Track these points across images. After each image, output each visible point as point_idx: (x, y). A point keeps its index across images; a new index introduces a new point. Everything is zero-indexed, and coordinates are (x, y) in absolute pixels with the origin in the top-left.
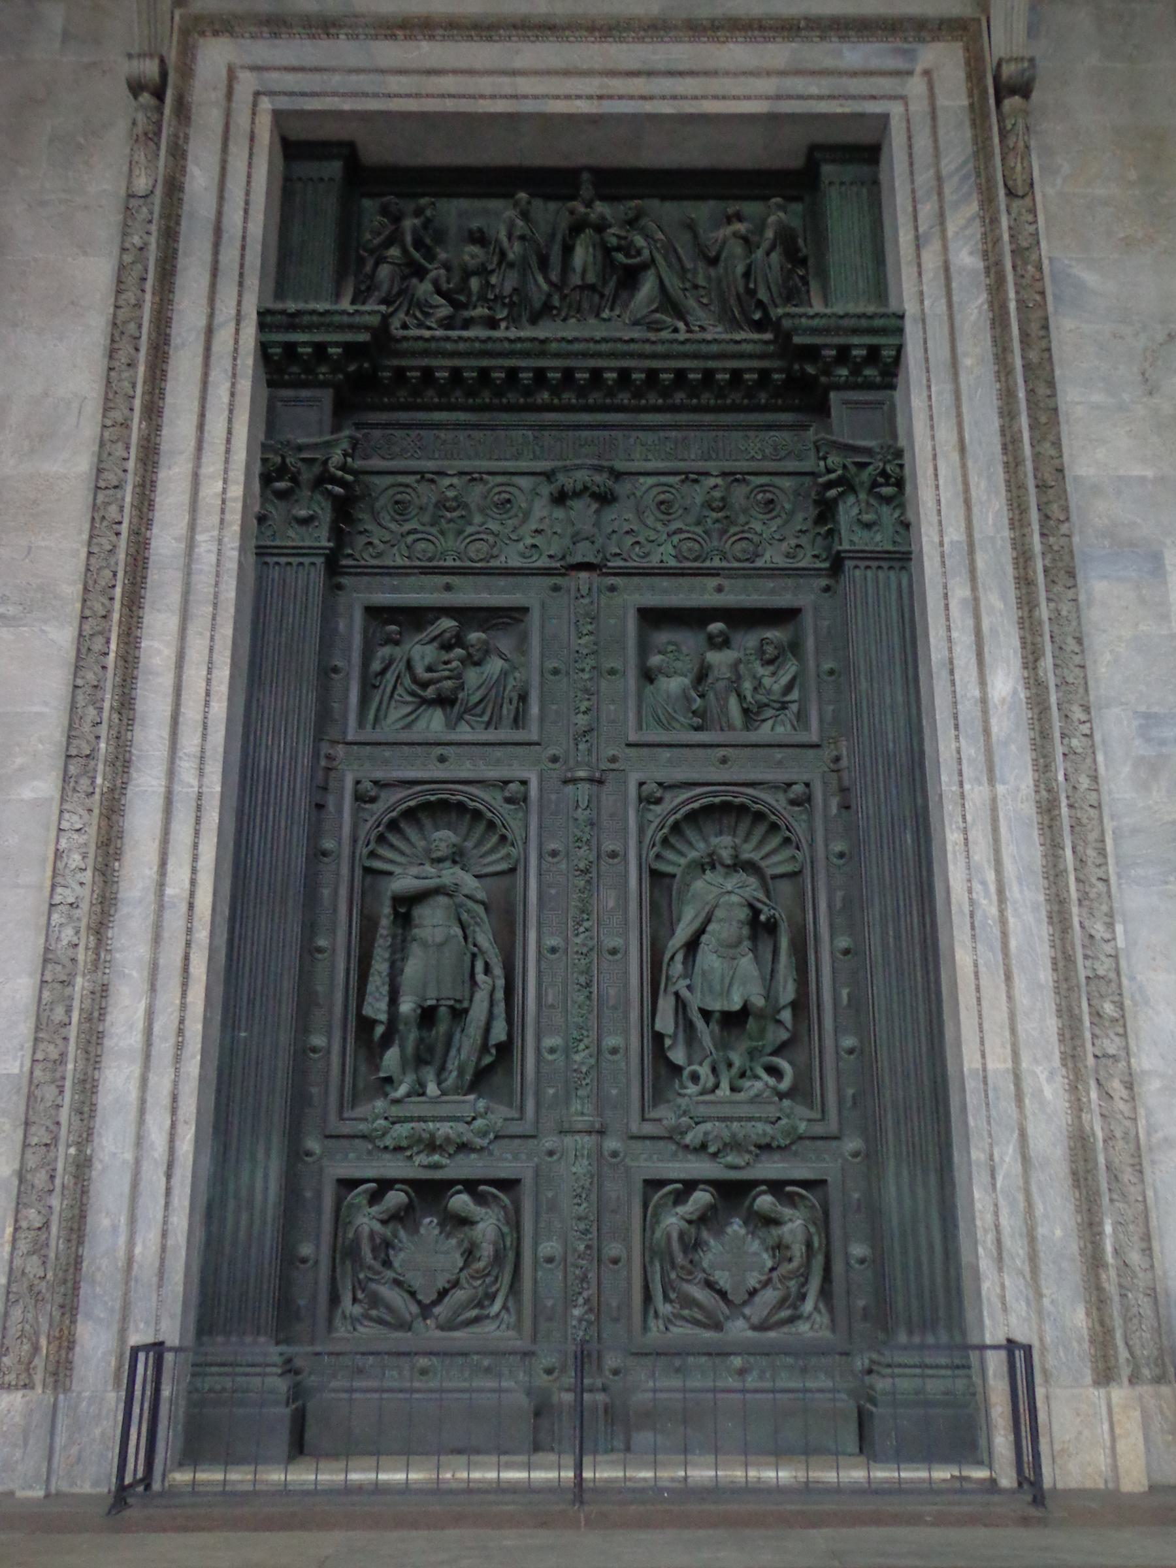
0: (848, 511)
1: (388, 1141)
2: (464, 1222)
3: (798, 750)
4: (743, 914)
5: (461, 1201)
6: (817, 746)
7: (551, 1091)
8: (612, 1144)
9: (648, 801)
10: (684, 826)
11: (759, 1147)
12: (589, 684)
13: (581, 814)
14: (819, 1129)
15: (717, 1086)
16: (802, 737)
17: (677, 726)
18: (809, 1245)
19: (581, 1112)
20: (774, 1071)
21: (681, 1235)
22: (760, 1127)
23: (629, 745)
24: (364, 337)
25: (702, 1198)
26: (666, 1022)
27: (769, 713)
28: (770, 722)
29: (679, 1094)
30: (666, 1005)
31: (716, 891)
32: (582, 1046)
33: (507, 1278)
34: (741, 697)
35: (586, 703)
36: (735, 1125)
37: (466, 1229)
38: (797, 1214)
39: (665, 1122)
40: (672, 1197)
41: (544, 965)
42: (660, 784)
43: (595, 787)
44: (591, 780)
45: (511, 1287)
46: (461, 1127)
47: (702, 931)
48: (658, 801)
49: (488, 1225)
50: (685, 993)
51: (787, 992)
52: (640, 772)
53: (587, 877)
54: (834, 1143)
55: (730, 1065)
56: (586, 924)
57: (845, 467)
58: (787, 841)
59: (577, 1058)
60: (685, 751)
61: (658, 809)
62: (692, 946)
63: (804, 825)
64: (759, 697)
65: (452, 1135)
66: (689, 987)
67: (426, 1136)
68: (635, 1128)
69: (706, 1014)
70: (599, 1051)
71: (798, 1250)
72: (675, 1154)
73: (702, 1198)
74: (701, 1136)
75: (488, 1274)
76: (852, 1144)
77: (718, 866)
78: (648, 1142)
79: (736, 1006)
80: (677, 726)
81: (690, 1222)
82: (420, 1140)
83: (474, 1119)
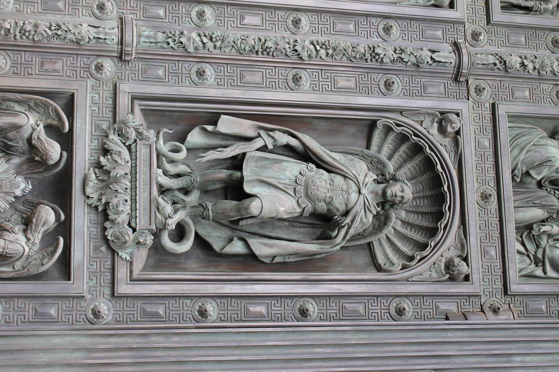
3: (500, 272)
4: (339, 204)
6: (506, 292)
7: (161, 12)
8: (109, 65)
9: (442, 120)
10: (418, 159)
12: (548, 69)
13: (426, 55)
14: (122, 272)
15: (165, 173)
16: (513, 274)
17: (515, 152)
19: (141, 35)
20: (180, 233)
21: (17, 127)
22: (127, 208)
23: (493, 105)
26: (227, 125)
27: (531, 247)
28: (522, 249)
29: (158, 133)
30: (246, 127)
31: (361, 179)
32: (205, 40)
34: (543, 221)
35: (530, 66)
36: (127, 183)
38: (36, 248)
39: (130, 116)
40: (55, 123)
41: (281, 13)
42: (458, 133)
43: (451, 69)
44: (459, 66)
47: (321, 164)
48: (442, 130)
50: (259, 143)
51: (262, 248)
52: (469, 117)
53: (368, 56)
54: (107, 291)
55: (186, 191)
56: (323, 52)
58: (411, 258)
59: (194, 35)
60: (491, 159)
61: (434, 130)
62: (305, 155)
63: (426, 275)
64: (545, 238)
66: (264, 149)
68: (127, 88)
69: (237, 163)
70: (201, 59)
72: (98, 127)
73: (54, 150)
74: (119, 149)
76: (104, 307)
77: (382, 186)
78: (110, 102)
79: (248, 189)
80: (515, 152)
81: (29, 140)
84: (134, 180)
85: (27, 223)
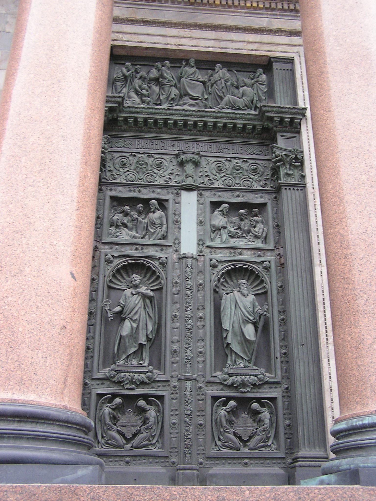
0: (282, 171)
1: (115, 379)
2: (143, 411)
5: (142, 403)
11: (252, 385)
18: (271, 420)
21: (225, 416)
24: (116, 105)
25: (232, 403)
33: (159, 431)
37: (143, 414)
45: (160, 434)
46: (143, 375)
49: (152, 413)
57: (282, 155)
65: (139, 378)
67: (129, 377)
71: (267, 421)
73: (232, 403)
75: (151, 428)
82: (128, 379)
83: (147, 372)
84: (243, 375)
85: (259, 413)
